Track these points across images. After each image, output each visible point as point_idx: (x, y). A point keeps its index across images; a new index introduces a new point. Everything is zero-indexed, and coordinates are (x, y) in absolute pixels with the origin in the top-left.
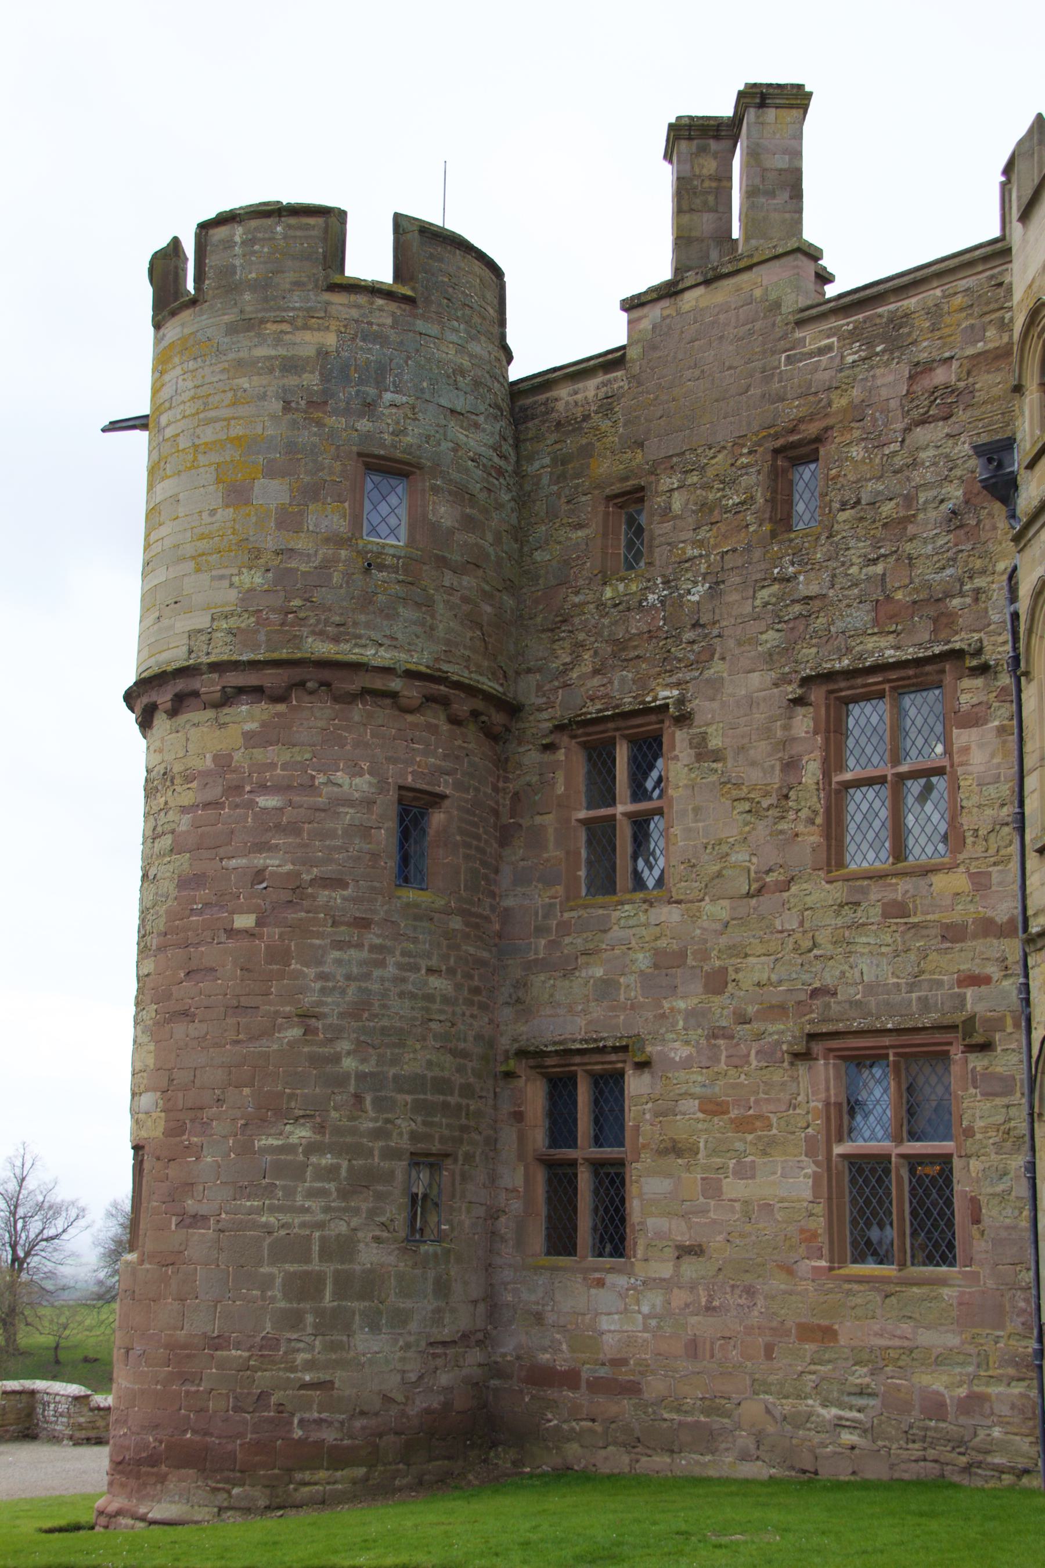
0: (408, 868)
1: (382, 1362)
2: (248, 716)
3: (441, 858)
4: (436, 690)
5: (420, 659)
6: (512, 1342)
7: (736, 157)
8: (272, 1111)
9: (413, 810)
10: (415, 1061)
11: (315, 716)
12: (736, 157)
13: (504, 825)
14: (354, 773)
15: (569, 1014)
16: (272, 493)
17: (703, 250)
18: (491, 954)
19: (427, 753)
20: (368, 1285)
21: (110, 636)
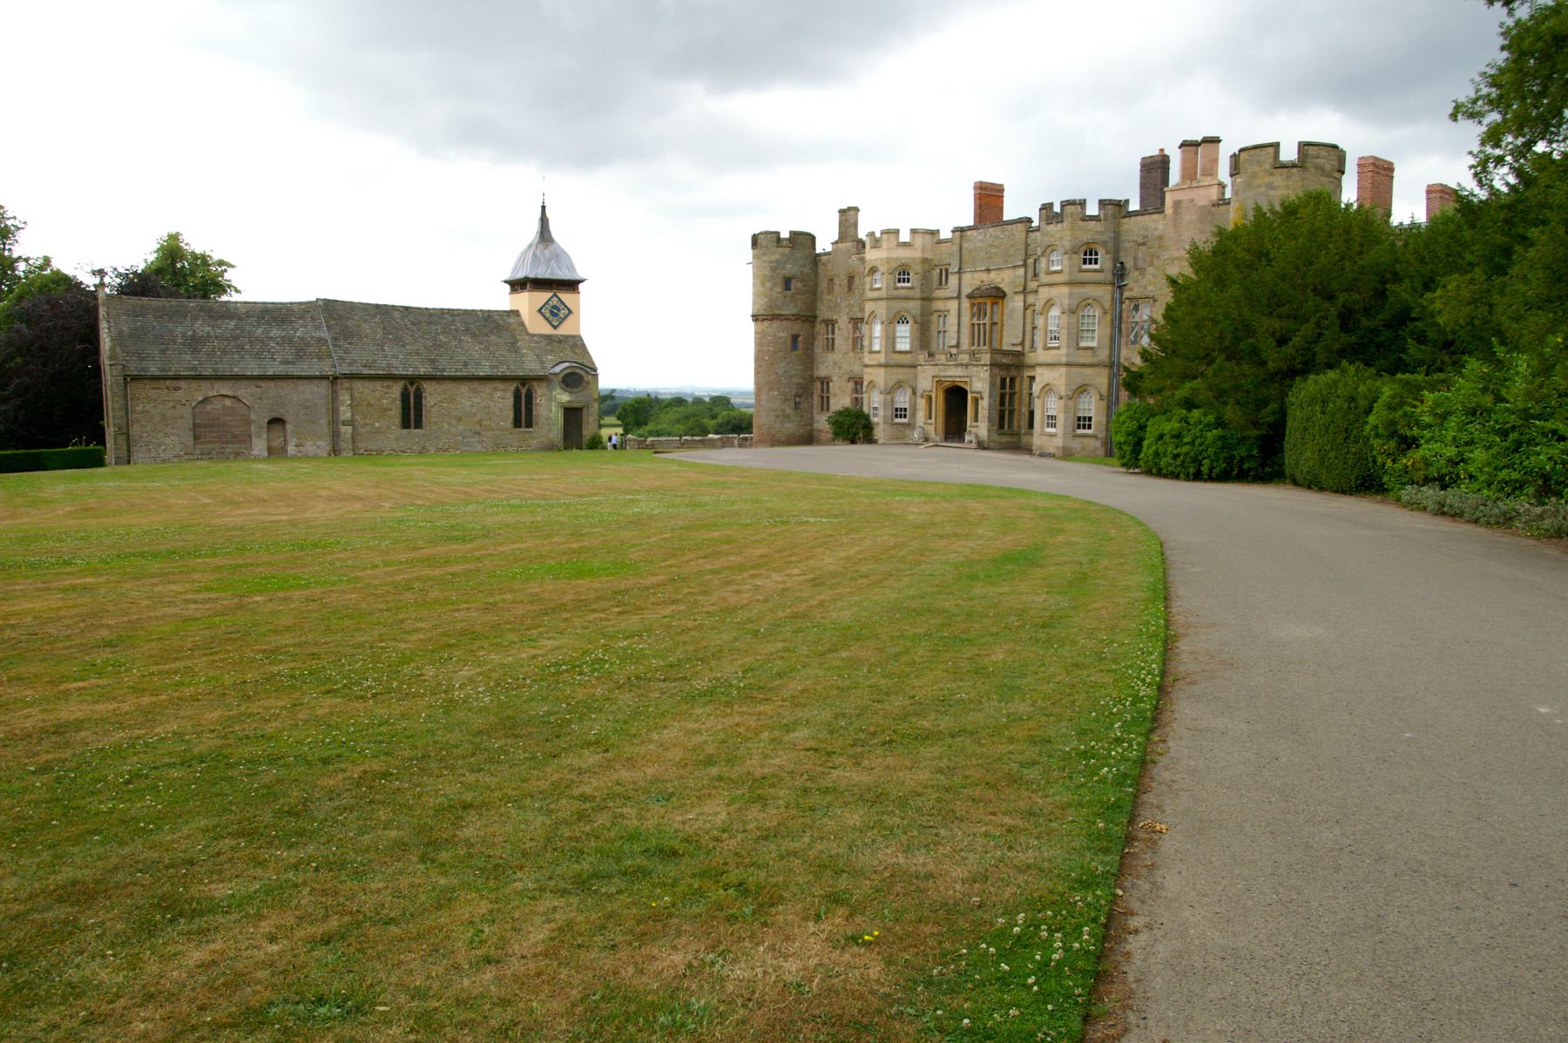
0: (794, 346)
1: (790, 427)
2: (766, 323)
3: (800, 345)
4: (797, 317)
5: (794, 311)
6: (816, 426)
7: (848, 217)
8: (771, 389)
9: (795, 338)
10: (795, 380)
11: (776, 324)
12: (848, 217)
13: (812, 337)
14: (782, 332)
15: (821, 372)
16: (768, 285)
17: (843, 237)
18: (809, 361)
19: (796, 328)
20: (787, 417)
21: (747, 308)
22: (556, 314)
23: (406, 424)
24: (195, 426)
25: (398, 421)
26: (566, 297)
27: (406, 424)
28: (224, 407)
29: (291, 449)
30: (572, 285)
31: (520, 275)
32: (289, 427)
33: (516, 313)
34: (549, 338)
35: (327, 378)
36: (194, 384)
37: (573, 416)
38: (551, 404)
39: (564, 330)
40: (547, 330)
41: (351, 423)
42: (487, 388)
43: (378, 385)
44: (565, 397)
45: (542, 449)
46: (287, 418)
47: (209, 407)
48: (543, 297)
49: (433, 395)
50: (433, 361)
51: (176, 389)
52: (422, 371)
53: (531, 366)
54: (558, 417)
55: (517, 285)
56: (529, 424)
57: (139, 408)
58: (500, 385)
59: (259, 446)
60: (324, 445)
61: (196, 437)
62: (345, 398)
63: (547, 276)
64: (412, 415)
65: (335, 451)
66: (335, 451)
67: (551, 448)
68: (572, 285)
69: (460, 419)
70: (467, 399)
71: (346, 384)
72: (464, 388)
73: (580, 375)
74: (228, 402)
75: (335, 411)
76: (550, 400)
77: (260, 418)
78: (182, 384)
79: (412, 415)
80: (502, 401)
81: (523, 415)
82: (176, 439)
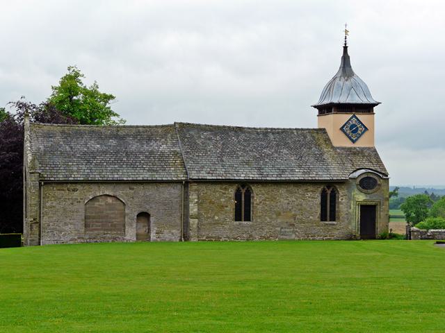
22: (354, 131)
23: (238, 218)
24: (86, 218)
25: (232, 215)
26: (362, 117)
27: (238, 218)
28: (107, 204)
29: (153, 236)
30: (368, 108)
31: (326, 102)
32: (152, 219)
33: (323, 131)
34: (350, 149)
35: (179, 182)
36: (86, 187)
37: (368, 212)
38: (351, 203)
39: (361, 143)
40: (348, 144)
41: (197, 217)
42: (301, 190)
43: (218, 188)
44: (361, 197)
45: (343, 239)
46: (150, 212)
47: (97, 204)
48: (344, 118)
49: (259, 196)
50: (259, 169)
51: (74, 190)
52: (254, 175)
53: (335, 172)
54: (356, 213)
55: (324, 109)
56: (333, 218)
57: (48, 204)
58: (310, 188)
59: (131, 233)
60: (177, 233)
61: (86, 226)
62: (193, 197)
63: (349, 101)
64: (243, 211)
65: (185, 237)
66: (185, 237)
67: (351, 238)
68: (368, 108)
69: (279, 214)
70: (284, 197)
71: (195, 187)
72: (282, 190)
73: (373, 180)
74: (110, 200)
75: (186, 207)
76: (350, 199)
77: (132, 212)
78: (78, 187)
79: (243, 211)
80: (314, 199)
81: (329, 211)
82: (73, 227)
